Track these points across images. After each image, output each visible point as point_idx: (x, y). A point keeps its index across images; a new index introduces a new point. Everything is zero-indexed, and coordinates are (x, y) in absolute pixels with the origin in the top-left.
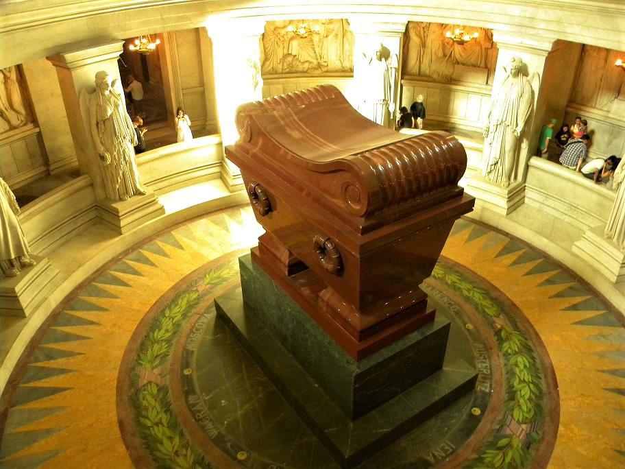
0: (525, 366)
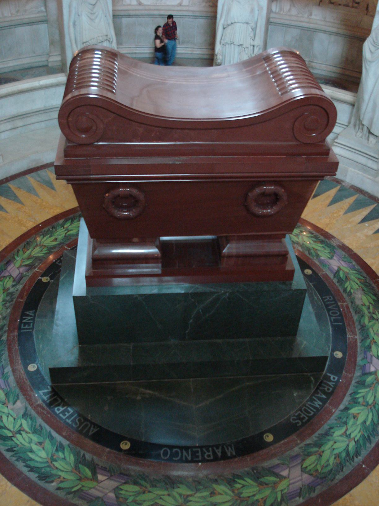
0: (31, 451)
